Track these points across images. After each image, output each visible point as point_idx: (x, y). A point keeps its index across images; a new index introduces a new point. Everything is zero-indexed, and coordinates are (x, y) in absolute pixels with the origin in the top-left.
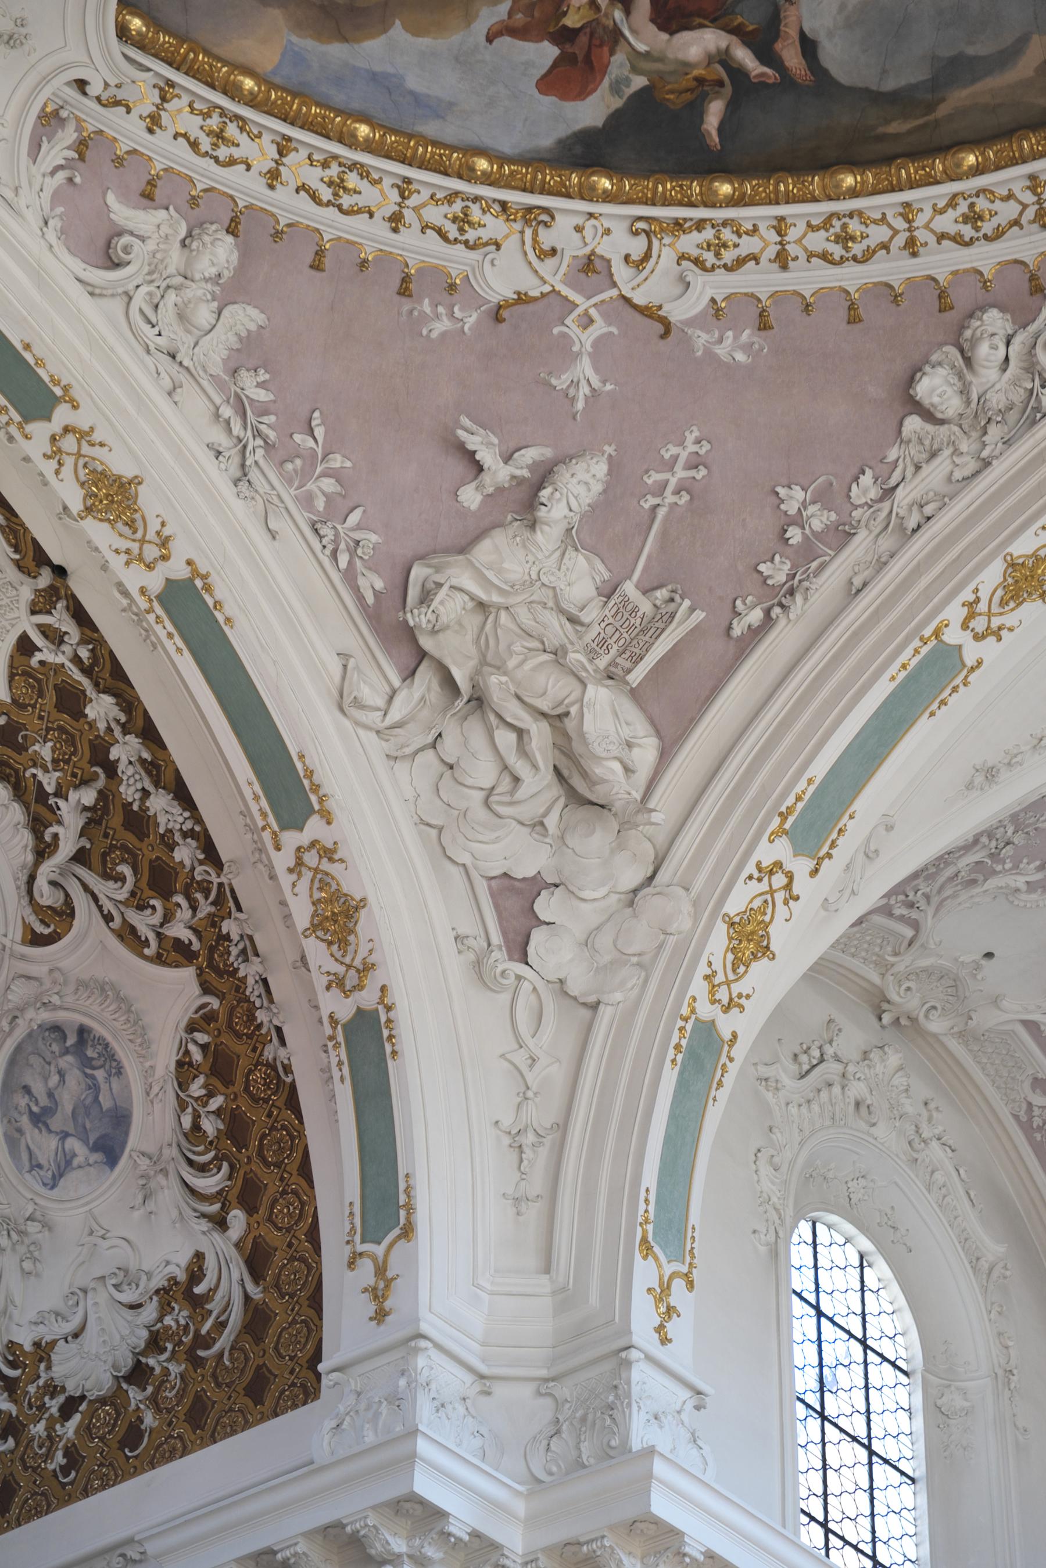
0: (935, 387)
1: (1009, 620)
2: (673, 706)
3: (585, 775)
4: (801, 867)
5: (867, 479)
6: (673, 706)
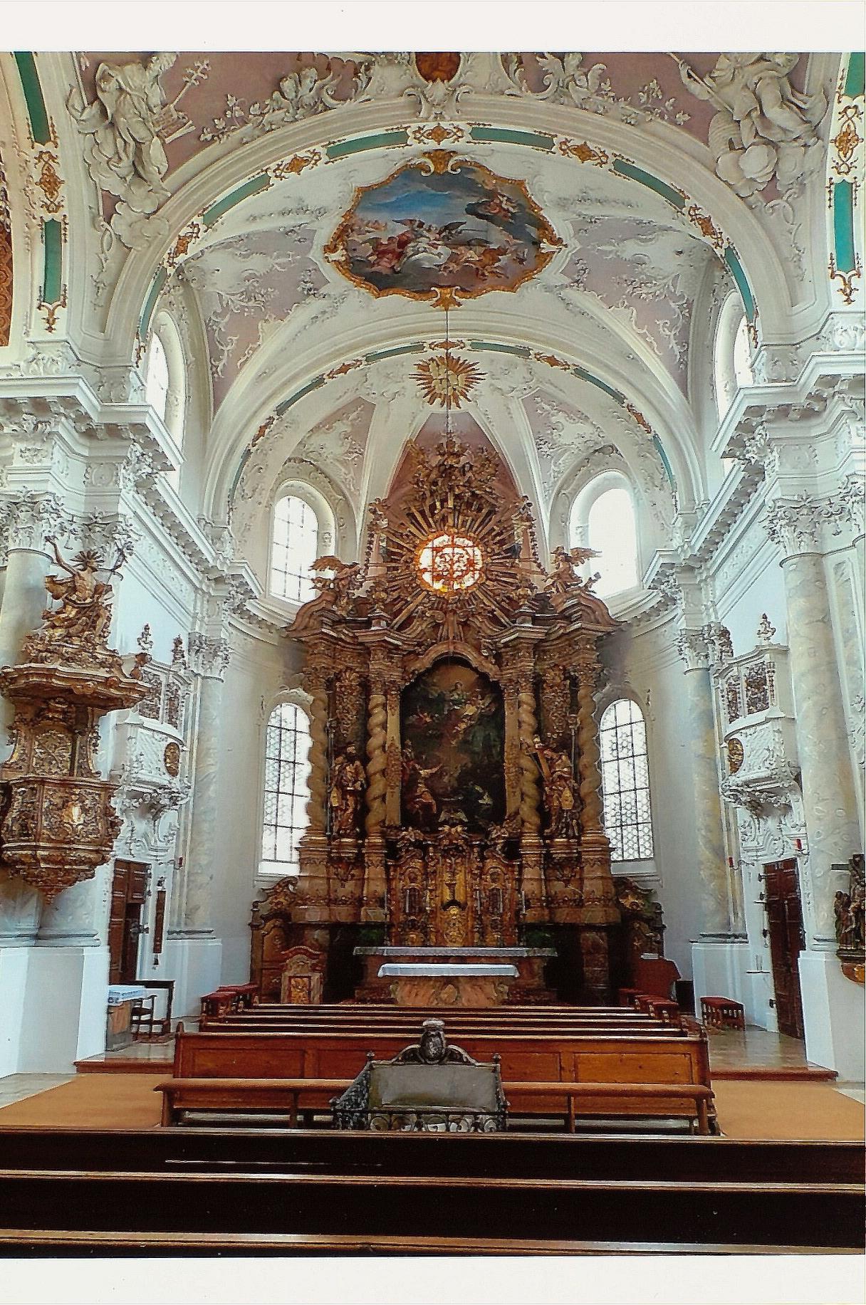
0: (287, 85)
1: (286, 175)
2: (177, 155)
3: (143, 167)
4: (203, 227)
5: (257, 106)
6: (177, 155)
